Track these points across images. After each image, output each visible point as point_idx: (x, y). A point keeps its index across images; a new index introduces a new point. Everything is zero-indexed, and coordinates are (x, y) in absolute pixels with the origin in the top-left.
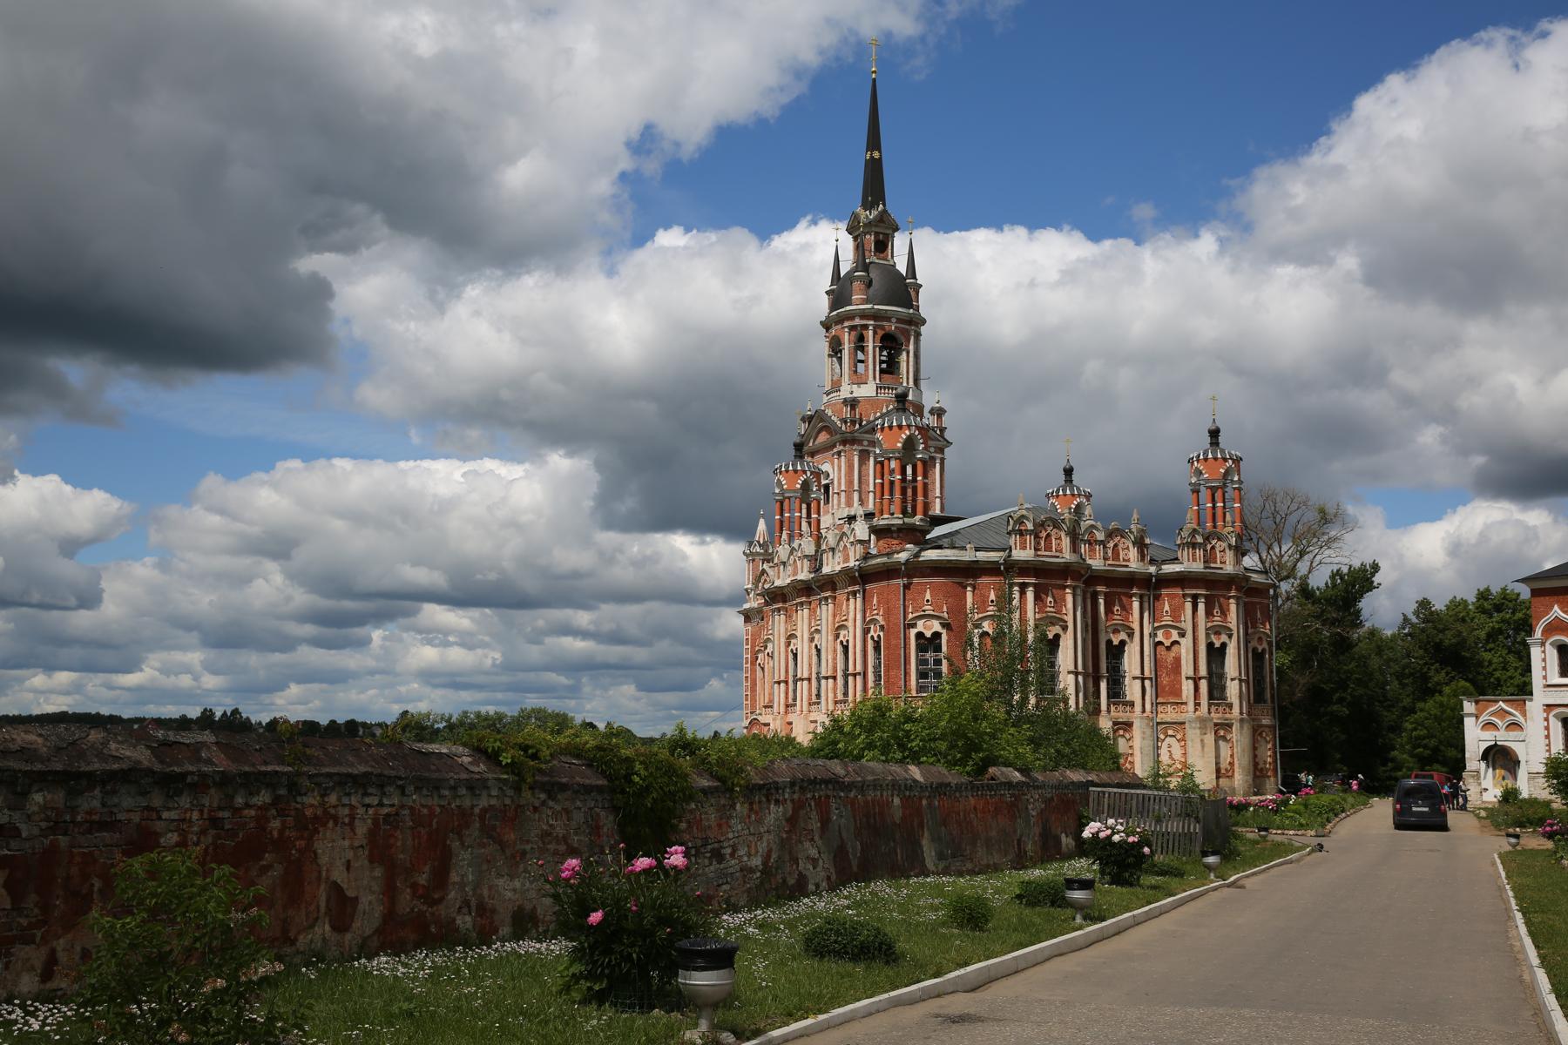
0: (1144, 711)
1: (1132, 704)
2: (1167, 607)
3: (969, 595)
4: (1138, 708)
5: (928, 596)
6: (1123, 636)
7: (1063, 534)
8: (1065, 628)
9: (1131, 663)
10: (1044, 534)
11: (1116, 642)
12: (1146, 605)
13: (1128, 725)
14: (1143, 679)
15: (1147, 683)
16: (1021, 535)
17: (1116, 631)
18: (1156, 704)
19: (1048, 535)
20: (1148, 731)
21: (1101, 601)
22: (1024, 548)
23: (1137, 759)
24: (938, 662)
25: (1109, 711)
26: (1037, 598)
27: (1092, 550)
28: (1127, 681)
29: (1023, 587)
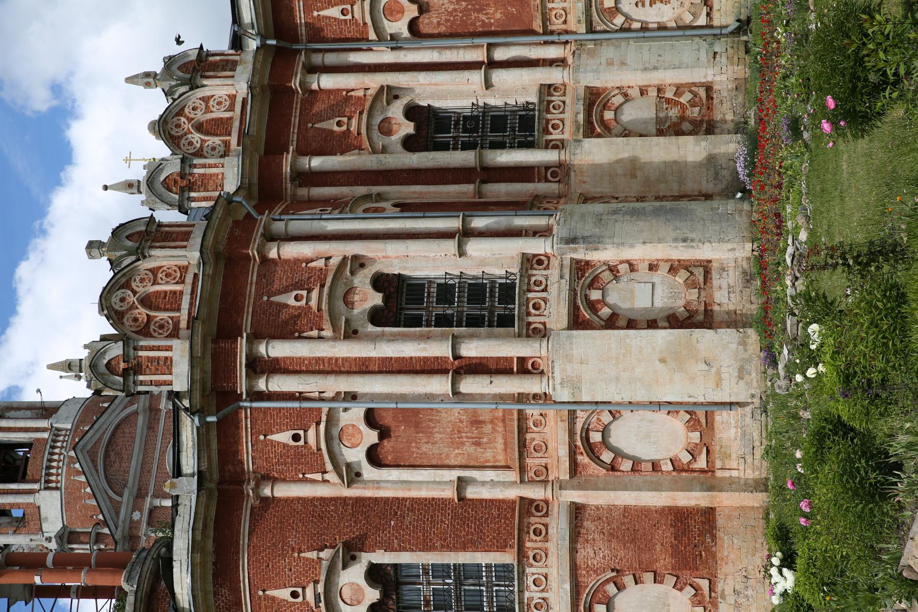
0: (560, 62)
1: (547, 89)
2: (334, 12)
3: (283, 491)
4: (554, 76)
5: (284, 594)
6: (396, 111)
7: (145, 265)
8: (359, 262)
9: (455, 93)
10: (142, 312)
11: (408, 128)
12: (331, 59)
13: (594, 99)
14: (493, 64)
15: (500, 54)
16: (138, 369)
17: (386, 128)
18: (548, 35)
19: (147, 301)
20: (607, 52)
21: (316, 162)
22: (167, 365)
23: (669, 77)
24: (441, 571)
25: (559, 146)
26: (289, 329)
27: (204, 183)
28: (495, 101)
29: (260, 367)
